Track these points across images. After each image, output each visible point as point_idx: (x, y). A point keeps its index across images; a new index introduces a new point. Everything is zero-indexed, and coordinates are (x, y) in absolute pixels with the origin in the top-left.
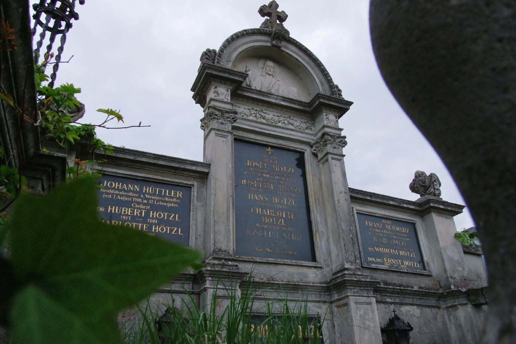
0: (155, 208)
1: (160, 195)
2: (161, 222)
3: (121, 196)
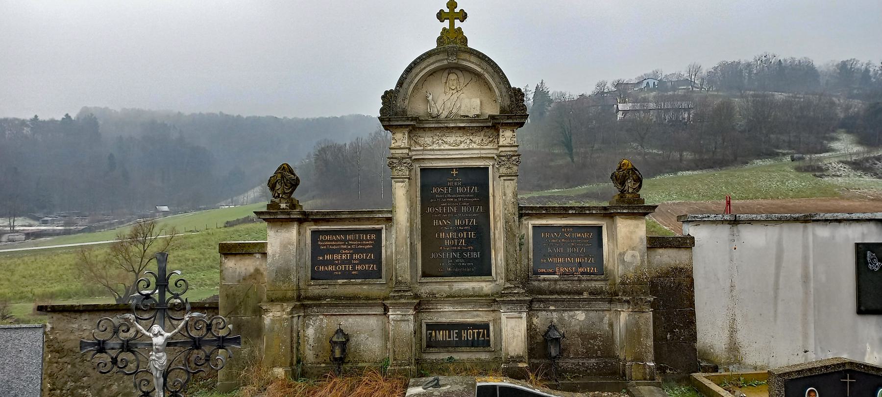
0: (357, 251)
1: (359, 240)
2: (362, 262)
3: (333, 245)
